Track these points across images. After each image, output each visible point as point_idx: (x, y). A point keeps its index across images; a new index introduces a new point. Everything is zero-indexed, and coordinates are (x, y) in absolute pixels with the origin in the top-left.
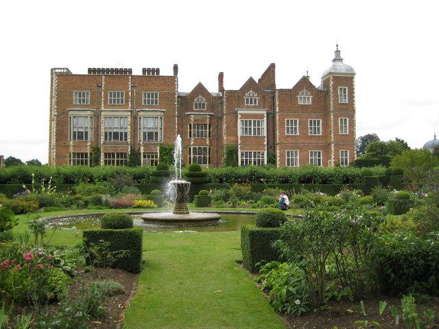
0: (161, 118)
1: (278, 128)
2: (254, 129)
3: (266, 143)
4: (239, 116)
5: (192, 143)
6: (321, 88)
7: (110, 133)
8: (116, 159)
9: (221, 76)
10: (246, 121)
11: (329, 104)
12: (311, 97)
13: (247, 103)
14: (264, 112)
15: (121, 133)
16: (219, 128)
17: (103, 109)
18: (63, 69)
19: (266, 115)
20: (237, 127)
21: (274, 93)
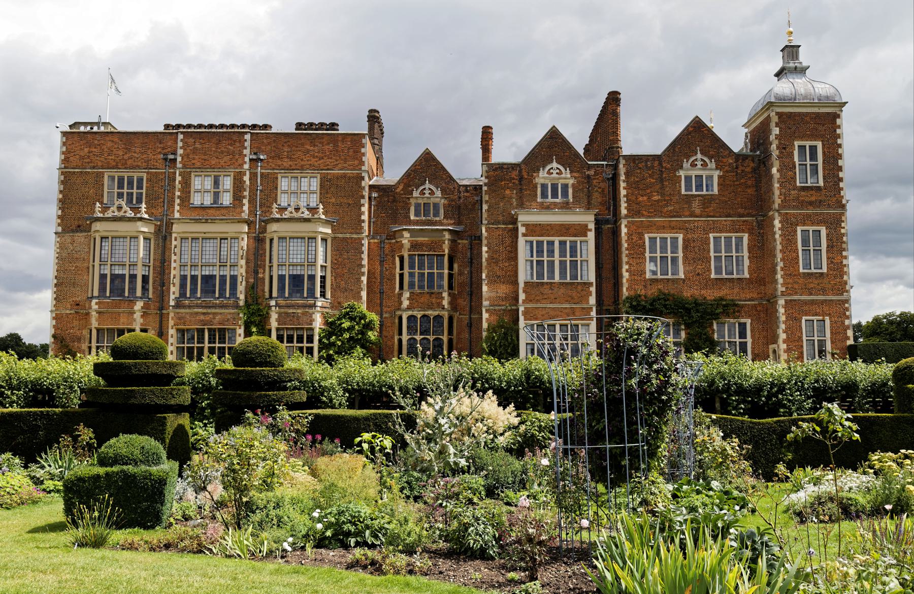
0: (324, 240)
1: (625, 259)
2: (563, 264)
3: (592, 300)
4: (522, 230)
5: (406, 303)
6: (747, 151)
7: (194, 278)
8: (207, 345)
9: (487, 134)
10: (540, 243)
11: (770, 190)
12: (716, 174)
13: (544, 195)
14: (589, 219)
15: (223, 278)
16: (474, 261)
17: (177, 215)
18: (98, 124)
19: (592, 226)
20: (515, 258)
21: (616, 167)
